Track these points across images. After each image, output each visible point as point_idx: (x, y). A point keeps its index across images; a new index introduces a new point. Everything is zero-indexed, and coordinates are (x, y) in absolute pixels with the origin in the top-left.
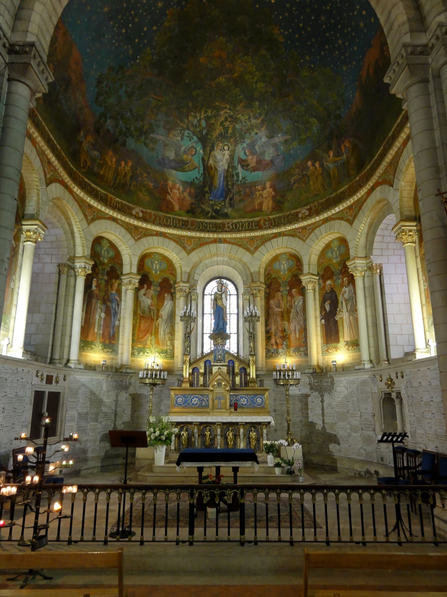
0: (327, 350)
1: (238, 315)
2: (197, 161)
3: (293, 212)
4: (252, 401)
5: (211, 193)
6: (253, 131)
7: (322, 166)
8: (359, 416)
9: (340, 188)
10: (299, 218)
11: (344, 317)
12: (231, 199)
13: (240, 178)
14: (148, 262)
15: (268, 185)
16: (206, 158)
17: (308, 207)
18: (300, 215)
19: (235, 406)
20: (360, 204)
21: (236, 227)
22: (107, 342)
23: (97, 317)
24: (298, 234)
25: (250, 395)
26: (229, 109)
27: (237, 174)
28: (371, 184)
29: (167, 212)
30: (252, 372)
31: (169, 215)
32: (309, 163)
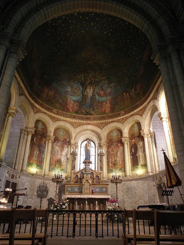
0: (133, 169)
1: (95, 155)
2: (79, 92)
3: (118, 113)
4: (101, 190)
5: (85, 105)
6: (102, 82)
7: (129, 95)
8: (148, 196)
9: (137, 103)
10: (120, 115)
11: (140, 155)
12: (93, 108)
13: (97, 100)
14: (58, 132)
15: (108, 103)
16: (83, 92)
17: (124, 111)
18: (121, 114)
20: (145, 108)
21: (95, 118)
22: (39, 164)
23: (35, 153)
24: (120, 121)
25: (100, 187)
26: (93, 73)
27: (96, 98)
28: (148, 100)
29: (67, 112)
31: (68, 113)
32: (124, 94)
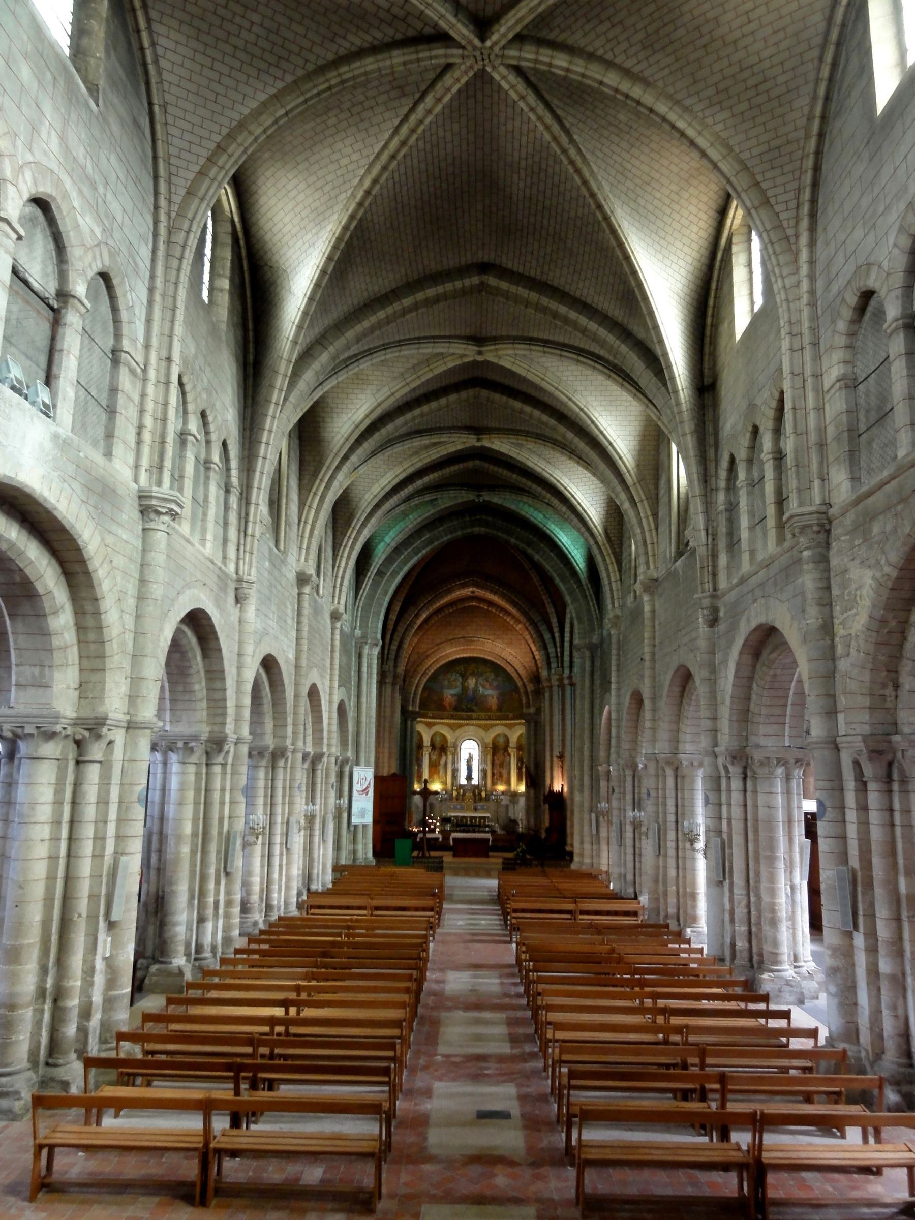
2: (459, 684)
19: (476, 810)
30: (483, 794)
